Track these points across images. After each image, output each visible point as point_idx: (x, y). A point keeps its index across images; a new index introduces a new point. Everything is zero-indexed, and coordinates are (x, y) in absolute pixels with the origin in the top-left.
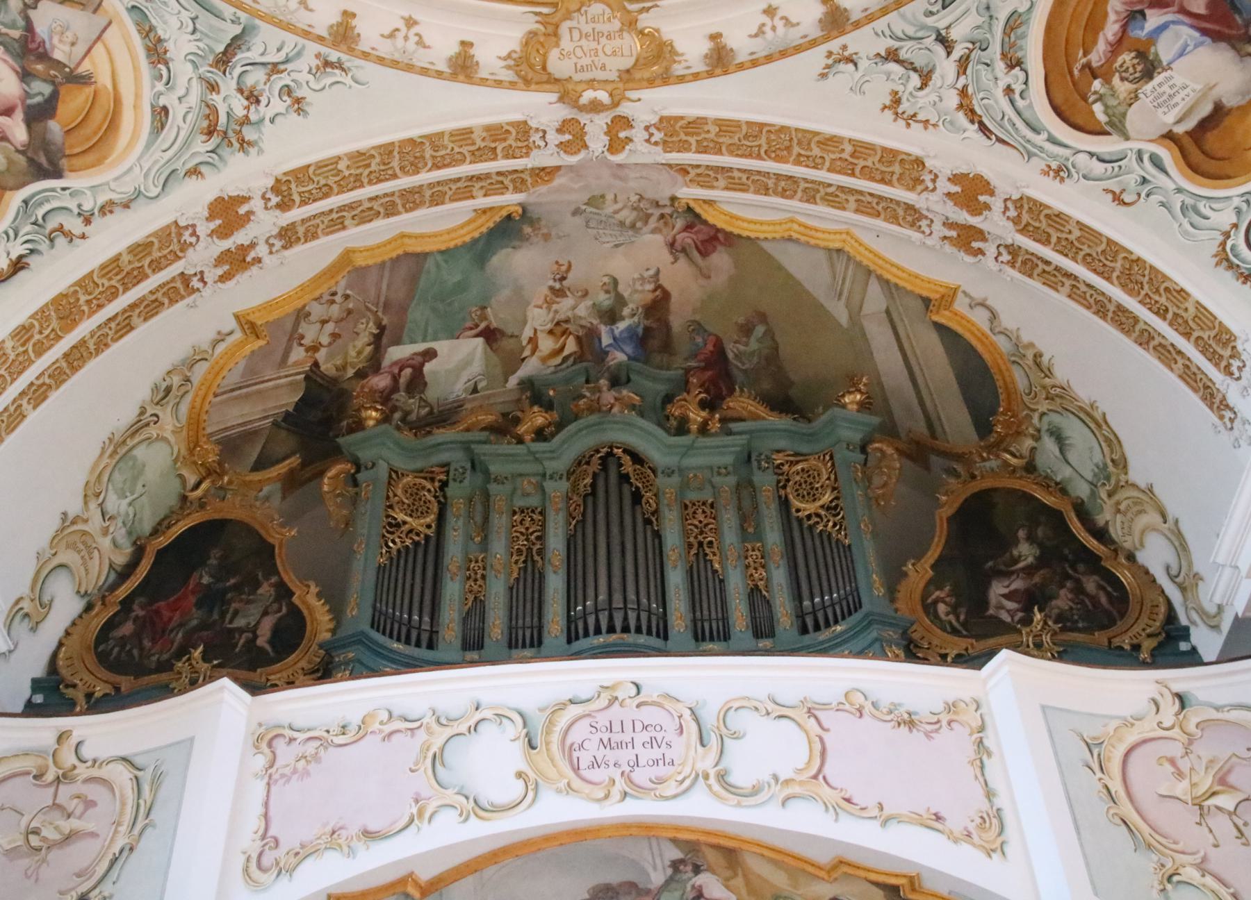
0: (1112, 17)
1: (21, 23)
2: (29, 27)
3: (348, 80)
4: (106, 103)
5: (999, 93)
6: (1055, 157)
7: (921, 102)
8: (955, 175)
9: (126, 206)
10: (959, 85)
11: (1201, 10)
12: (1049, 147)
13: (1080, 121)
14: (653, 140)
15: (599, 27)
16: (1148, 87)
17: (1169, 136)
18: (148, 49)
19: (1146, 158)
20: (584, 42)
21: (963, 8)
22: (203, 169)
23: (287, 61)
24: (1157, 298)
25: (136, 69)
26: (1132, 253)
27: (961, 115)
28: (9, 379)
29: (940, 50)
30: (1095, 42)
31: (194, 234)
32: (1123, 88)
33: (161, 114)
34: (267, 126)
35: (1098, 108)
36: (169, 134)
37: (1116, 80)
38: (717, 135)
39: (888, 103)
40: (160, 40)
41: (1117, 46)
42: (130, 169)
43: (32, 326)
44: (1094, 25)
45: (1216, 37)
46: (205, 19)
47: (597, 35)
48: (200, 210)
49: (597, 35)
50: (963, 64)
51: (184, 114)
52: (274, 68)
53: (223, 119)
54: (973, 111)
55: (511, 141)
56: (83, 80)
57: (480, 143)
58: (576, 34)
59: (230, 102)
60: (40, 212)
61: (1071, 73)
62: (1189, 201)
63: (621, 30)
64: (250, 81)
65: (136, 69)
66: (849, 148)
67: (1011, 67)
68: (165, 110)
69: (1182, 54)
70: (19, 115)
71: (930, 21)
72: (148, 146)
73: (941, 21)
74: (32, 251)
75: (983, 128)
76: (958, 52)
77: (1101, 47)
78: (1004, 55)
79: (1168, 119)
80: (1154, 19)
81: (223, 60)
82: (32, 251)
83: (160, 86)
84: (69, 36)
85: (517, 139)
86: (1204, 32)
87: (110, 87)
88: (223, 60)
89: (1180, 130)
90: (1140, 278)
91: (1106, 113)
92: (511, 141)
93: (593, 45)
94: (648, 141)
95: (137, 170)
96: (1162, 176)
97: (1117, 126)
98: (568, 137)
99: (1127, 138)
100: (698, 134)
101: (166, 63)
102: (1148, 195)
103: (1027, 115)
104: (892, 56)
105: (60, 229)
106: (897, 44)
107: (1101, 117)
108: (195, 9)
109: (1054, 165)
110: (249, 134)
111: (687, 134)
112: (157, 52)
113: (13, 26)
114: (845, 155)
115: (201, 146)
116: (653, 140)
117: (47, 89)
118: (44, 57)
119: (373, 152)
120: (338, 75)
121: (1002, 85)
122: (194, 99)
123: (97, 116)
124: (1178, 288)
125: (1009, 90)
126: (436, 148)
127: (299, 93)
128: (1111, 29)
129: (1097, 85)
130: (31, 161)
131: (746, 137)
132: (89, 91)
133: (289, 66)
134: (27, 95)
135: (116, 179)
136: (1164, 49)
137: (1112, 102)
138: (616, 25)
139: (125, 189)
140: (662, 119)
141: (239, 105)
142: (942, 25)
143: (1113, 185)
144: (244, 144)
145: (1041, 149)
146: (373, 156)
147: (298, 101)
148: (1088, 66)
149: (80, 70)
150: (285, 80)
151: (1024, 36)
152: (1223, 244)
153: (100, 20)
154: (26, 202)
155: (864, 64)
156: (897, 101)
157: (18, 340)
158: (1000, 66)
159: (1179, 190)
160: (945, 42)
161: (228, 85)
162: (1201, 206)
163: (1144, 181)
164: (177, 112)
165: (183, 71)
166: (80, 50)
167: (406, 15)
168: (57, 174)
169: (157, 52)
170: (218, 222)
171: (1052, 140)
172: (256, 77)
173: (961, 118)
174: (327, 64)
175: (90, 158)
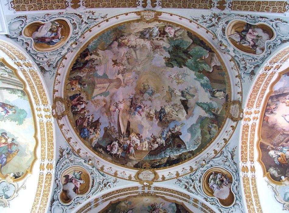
0: (60, 34)
1: (242, 41)
2: (241, 40)
3: (193, 17)
4: (235, 28)
5: (75, 20)
6: (62, 15)
7: (88, 15)
8: (80, 7)
9: (239, 15)
10: (82, 19)
11: (46, 39)
12: (64, 16)
13: (59, 21)
14: (138, 2)
15: (147, 17)
16: (50, 28)
17: (43, 25)
18: (225, 31)
19: (46, 21)
20: (150, 14)
21: (84, 28)
22: (223, 14)
23: (203, 23)
24: (34, 4)
25: (228, 29)
26: (42, 10)
27: (81, 15)
28: (275, 3)
29: (87, 22)
30: (61, 30)
31: (229, 5)
32: (54, 27)
33: (227, 23)
34: (210, 15)
35: (57, 23)
36: (227, 20)
37: (56, 27)
38: (125, 3)
39: (94, 13)
40: (222, 31)
41: (57, 32)
42: (235, 19)
43: (265, 9)
44: (62, 32)
45: (42, 38)
46: (214, 31)
47: (148, 15)
48: (226, 10)
49: (148, 15)
50: (82, 21)
51: (221, 24)
52: (205, 22)
53: (217, 19)
54: (79, 16)
55: (166, 3)
56: (236, 31)
57: (171, 4)
58: (152, 16)
59: (214, 21)
60: (254, 21)
61: (63, 25)
62: (36, 19)
63: (143, 16)
64: (210, 22)
65: (228, 29)
66: (100, 5)
67: (74, 23)
68: (226, 23)
69: (46, 34)
70: (249, 32)
71: (90, 25)
72: (231, 20)
73: (87, 25)
74: (258, 18)
75: (76, 14)
76: (84, 22)
77: (60, 30)
78: (76, 24)
79: (44, 26)
80: (53, 35)
81: (213, 25)
82: (258, 18)
83: (225, 26)
84: (236, 37)
85: (164, 3)
86: (45, 37)
87: (233, 30)
88: (213, 25)
89: (42, 26)
90: (38, 5)
91: (55, 23)
92: (166, 3)
93: (149, 14)
94: (139, 2)
95: (234, 18)
96: (42, 20)
97: (53, 23)
98: (154, 4)
99: (51, 22)
100: (130, 3)
101: (223, 28)
102: (43, 17)
103: (69, 18)
104: (95, 19)
105: (251, 18)
106: (95, 21)
107: (56, 22)
108: (215, 32)
109: (62, 14)
110: (213, 16)
111: (132, 3)
112: (223, 30)
113: (243, 41)
114: (101, 3)
115: (222, 17)
116: (138, 2)
117: (243, 33)
118: (241, 36)
119: (191, 7)
120: (195, 18)
121: (75, 21)
122: (220, 23)
123: (237, 27)
124: (31, 10)
125: (73, 20)
126: (180, 5)
127: (202, 18)
128: (59, 32)
129: (59, 26)
130: (251, 27)
131: (120, 4)
132: (237, 30)
133: (203, 22)
134: (246, 34)
135: (239, 19)
136: (50, 33)
137: (55, 24)
138: (144, 17)
139: (237, 17)
140: (136, 7)
141: (213, 19)
142: (87, 25)
143: (50, 16)
144: (215, 14)
145: (65, 15)
146: (192, 6)
147: (203, 17)
148: (61, 27)
149: (236, 33)
150: (204, 20)
151: (73, 27)
152: (26, 18)
153: (230, 36)
154: (255, 23)
155: (100, 17)
156: (92, 14)
157: (269, 9)
158: (76, 23)
159: (38, 20)
160: (85, 23)
161: (214, 22)
162: (33, 20)
163: (45, 18)
164: (224, 22)
165: (220, 27)
166: (235, 35)
167: (181, 20)
168: (247, 23)
169: (223, 30)
170: (224, 5)
171: (63, 17)
172: (209, 22)
173: (80, 14)
174: (196, 20)
175: (241, 23)
